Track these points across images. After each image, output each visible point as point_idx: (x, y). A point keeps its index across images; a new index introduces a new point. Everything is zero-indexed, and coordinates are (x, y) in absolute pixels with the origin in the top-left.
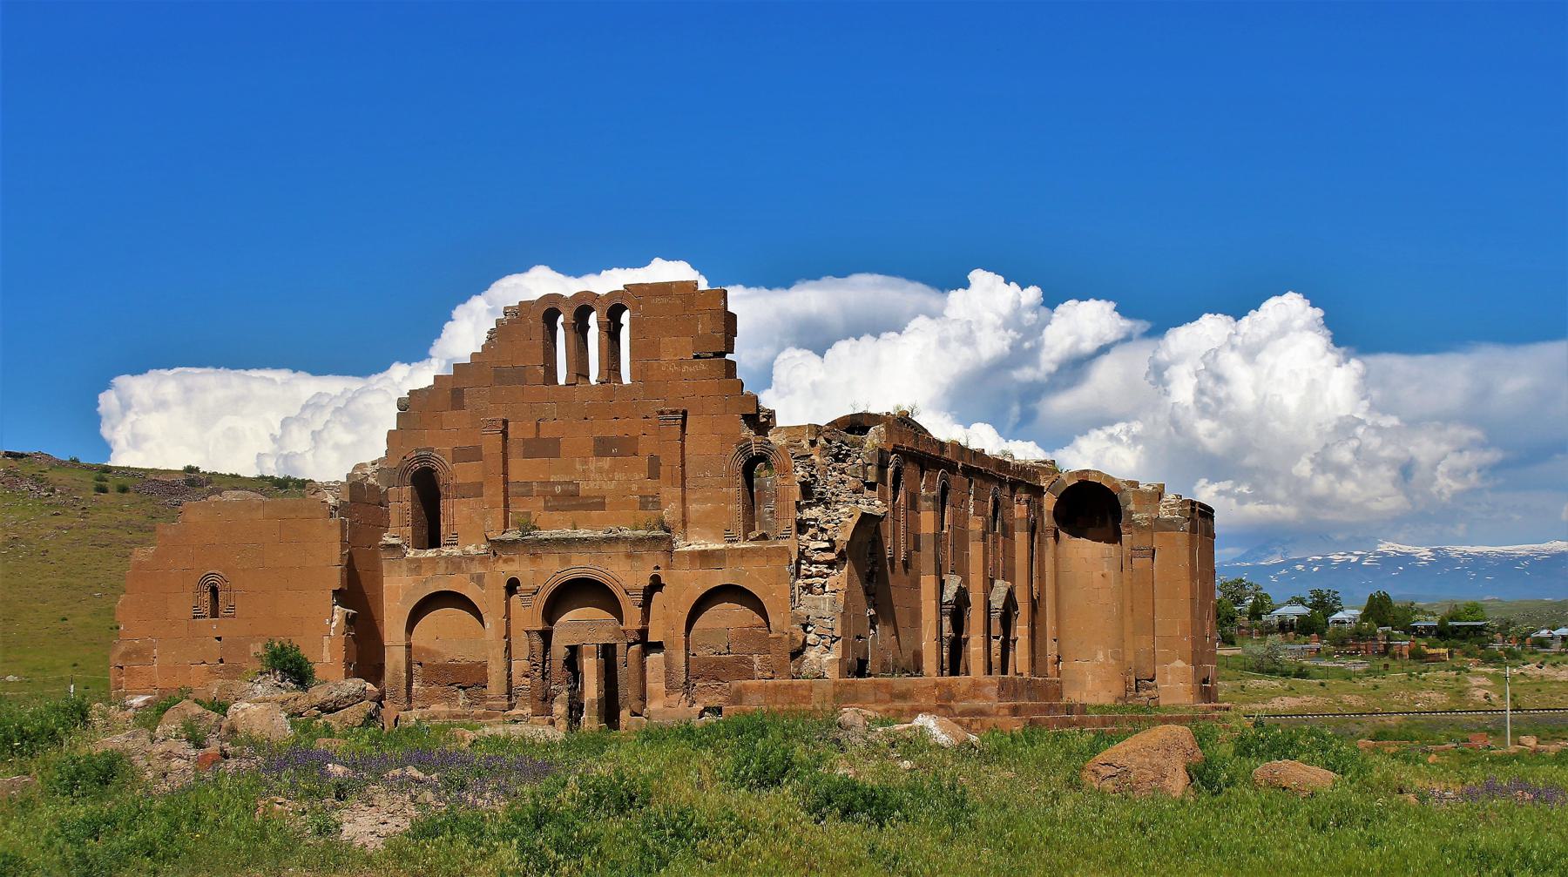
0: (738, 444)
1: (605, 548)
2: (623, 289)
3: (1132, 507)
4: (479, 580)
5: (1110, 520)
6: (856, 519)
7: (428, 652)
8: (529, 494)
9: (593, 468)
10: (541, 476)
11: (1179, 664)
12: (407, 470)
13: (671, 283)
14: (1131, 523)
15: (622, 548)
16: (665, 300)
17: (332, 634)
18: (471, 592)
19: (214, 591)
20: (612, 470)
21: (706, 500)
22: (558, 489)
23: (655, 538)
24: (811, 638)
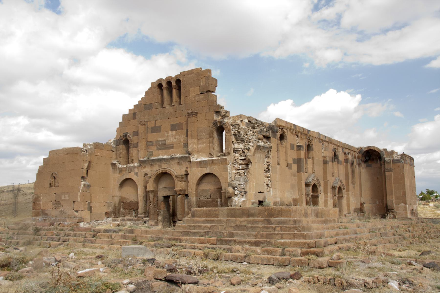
0: (213, 122)
1: (171, 162)
2: (180, 74)
3: (385, 156)
4: (137, 174)
5: (379, 160)
6: (255, 146)
7: (125, 198)
8: (152, 145)
9: (170, 135)
10: (156, 139)
11: (403, 204)
12: (121, 140)
13: (193, 69)
14: (384, 161)
15: (176, 161)
16: (191, 75)
17: (80, 191)
18: (134, 178)
19: (55, 178)
20: (175, 135)
21: (203, 143)
22: (160, 143)
23: (185, 157)
24: (236, 192)
